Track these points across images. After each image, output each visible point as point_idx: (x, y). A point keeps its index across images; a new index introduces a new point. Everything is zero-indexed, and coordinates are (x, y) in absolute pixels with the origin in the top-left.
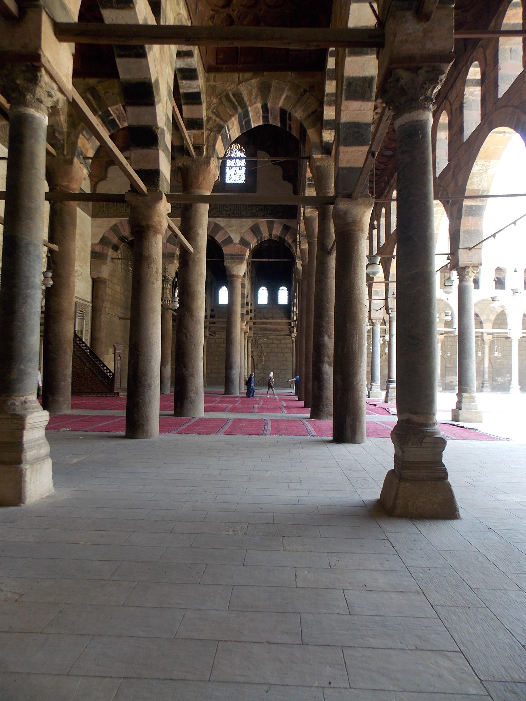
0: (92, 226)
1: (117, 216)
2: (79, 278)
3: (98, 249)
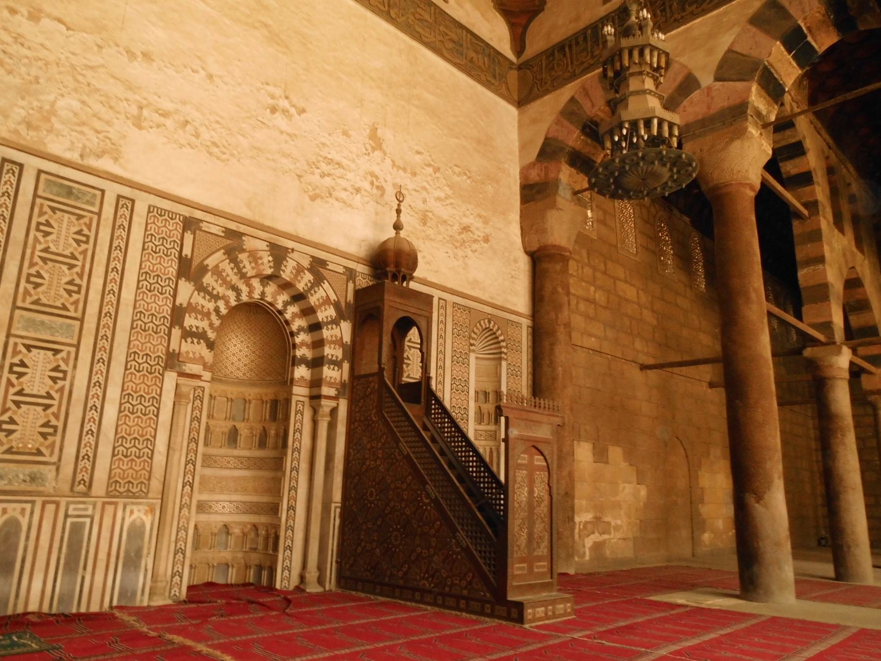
0: (520, 126)
1: (573, 77)
2: (475, 246)
3: (535, 176)
